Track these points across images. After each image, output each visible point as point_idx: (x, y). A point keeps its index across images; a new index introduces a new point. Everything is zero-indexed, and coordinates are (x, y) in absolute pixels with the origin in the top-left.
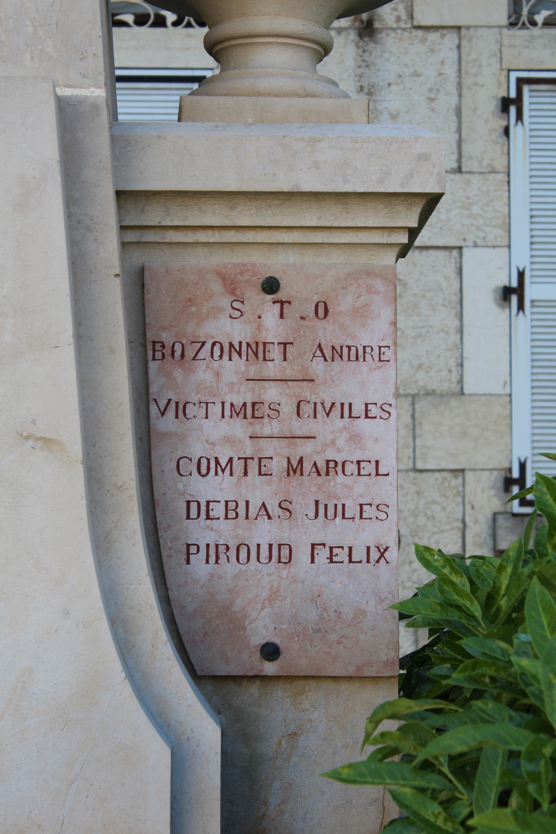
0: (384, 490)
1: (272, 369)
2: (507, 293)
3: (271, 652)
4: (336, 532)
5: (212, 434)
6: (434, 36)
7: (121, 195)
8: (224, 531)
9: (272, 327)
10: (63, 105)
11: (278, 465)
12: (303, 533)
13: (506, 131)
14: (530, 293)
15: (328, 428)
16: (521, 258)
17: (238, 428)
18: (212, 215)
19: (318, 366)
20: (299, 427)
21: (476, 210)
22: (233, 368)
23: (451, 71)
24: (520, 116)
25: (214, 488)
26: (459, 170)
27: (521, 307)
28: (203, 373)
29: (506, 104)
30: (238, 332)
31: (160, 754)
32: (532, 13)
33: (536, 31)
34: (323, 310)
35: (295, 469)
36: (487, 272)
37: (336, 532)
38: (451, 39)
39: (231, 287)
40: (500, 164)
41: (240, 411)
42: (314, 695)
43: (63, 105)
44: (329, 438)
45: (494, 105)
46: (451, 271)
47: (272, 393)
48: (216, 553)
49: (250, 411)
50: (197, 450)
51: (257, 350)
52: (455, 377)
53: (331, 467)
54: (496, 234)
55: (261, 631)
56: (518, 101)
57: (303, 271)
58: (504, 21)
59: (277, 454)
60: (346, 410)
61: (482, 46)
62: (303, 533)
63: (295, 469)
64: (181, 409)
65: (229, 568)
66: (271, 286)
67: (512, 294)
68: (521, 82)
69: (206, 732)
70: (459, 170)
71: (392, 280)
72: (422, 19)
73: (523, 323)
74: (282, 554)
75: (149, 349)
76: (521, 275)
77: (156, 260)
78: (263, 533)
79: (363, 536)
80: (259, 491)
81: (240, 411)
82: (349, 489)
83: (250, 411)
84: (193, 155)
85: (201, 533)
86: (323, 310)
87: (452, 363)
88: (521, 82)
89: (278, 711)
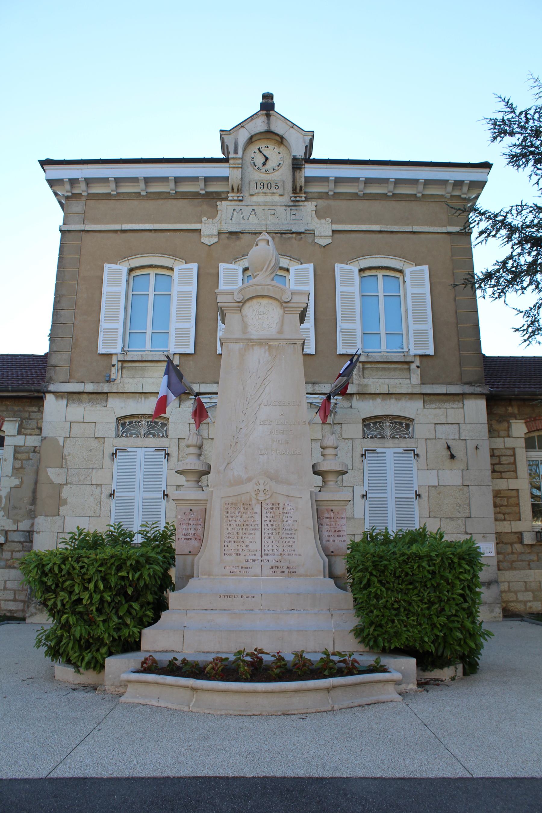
0: (345, 534)
1: (332, 520)
2: (363, 496)
3: (332, 552)
4: (340, 538)
5: (326, 527)
6: (347, 441)
7: (316, 501)
8: (327, 538)
9: (332, 515)
10: (311, 492)
11: (333, 531)
12: (336, 539)
13: (363, 461)
14: (368, 496)
15: (339, 527)
16: (366, 488)
17: (328, 527)
18: (325, 502)
19: (337, 520)
20: (335, 526)
21: (356, 478)
22: (328, 520)
23: (350, 448)
24: (365, 458)
25: (326, 534)
26: (353, 469)
27: (366, 499)
28: (324, 520)
29: (362, 455)
30: (328, 516)
31: (322, 562)
32: (368, 435)
33: (368, 439)
34: (338, 513)
35: (335, 531)
36: (359, 491)
37: (340, 538)
38: (350, 441)
39: (327, 511)
40: (361, 468)
41: (328, 525)
42: (337, 557)
43: (311, 492)
44: (339, 528)
45: (360, 455)
46: (351, 491)
47: (332, 523)
48: (326, 541)
49: (330, 525)
50: (324, 529)
51: (330, 518)
52: (352, 514)
53: (339, 531)
54: (361, 483)
55: (331, 550)
56: (365, 455)
57: (336, 509)
58: (362, 437)
59: (333, 530)
60: (341, 524)
61: (357, 443)
62: (336, 539)
63: (335, 531)
64: (322, 525)
65: (328, 542)
66: (332, 510)
67: (364, 496)
68: (365, 450)
69: (327, 560)
70: (353, 469)
71: (345, 509)
72: (344, 437)
73: (367, 503)
74: (334, 541)
75: (318, 518)
76: (366, 492)
77: (319, 508)
78: (331, 539)
79: (343, 539)
80: (331, 534)
81: (328, 525)
82: (341, 534)
83: (330, 525)
84: (324, 496)
85: (324, 539)
86: (338, 513)
87: (352, 511)
88: (365, 450)
89: (333, 559)
